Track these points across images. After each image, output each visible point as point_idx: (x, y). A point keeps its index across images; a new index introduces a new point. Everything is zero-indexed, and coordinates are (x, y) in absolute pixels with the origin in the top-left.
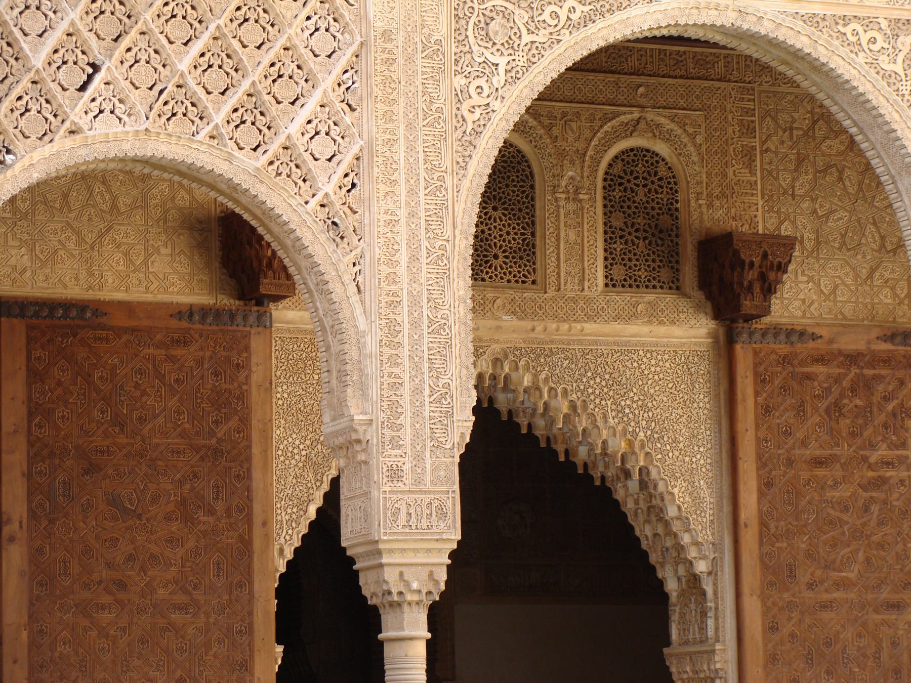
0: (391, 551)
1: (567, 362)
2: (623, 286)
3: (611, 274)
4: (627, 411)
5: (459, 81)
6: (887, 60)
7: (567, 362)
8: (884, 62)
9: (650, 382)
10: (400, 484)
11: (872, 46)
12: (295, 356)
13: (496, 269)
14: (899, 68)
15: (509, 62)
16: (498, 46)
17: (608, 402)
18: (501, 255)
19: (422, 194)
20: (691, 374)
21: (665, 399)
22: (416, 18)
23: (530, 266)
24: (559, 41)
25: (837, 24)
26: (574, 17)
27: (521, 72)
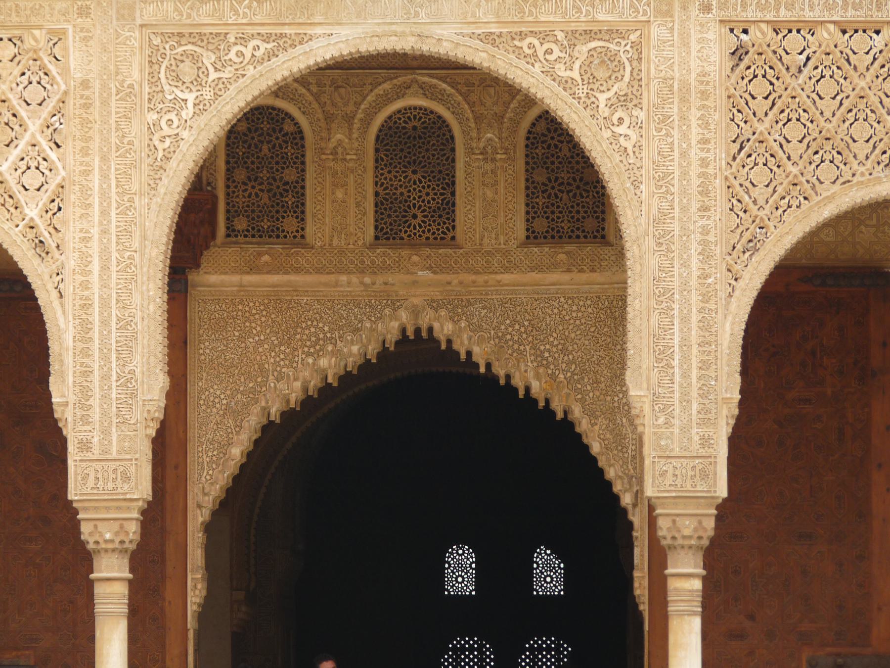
0: (86, 509)
1: (486, 311)
2: (545, 237)
3: (532, 227)
4: (546, 354)
5: (152, 117)
6: (563, 68)
7: (486, 311)
8: (561, 71)
9: (571, 327)
10: (89, 454)
11: (548, 57)
12: (217, 315)
13: (415, 228)
14: (576, 75)
15: (197, 97)
16: (188, 85)
17: (527, 347)
18: (420, 215)
19: (113, 214)
20: (615, 318)
21: (587, 342)
22: (112, 67)
23: (450, 224)
24: (244, 76)
25: (513, 39)
27: (208, 104)
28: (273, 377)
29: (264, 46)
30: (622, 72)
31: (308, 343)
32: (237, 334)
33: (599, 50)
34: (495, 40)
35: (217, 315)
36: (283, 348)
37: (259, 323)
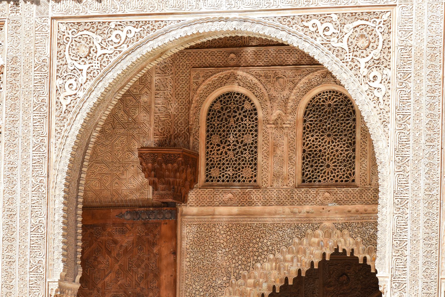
1: (374, 230)
8: (334, 42)
11: (326, 33)
12: (198, 235)
15: (89, 68)
25: (302, 21)
26: (130, 36)
27: (96, 73)
28: (234, 277)
29: (134, 30)
30: (376, 43)
31: (257, 254)
32: (211, 247)
33: (361, 27)
34: (290, 22)
35: (198, 235)
36: (240, 257)
37: (225, 240)
